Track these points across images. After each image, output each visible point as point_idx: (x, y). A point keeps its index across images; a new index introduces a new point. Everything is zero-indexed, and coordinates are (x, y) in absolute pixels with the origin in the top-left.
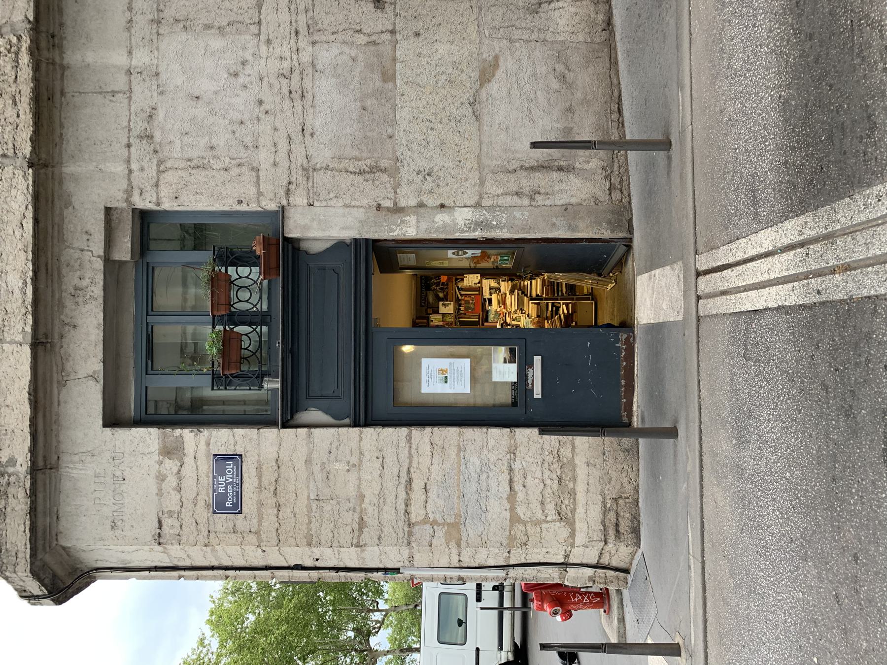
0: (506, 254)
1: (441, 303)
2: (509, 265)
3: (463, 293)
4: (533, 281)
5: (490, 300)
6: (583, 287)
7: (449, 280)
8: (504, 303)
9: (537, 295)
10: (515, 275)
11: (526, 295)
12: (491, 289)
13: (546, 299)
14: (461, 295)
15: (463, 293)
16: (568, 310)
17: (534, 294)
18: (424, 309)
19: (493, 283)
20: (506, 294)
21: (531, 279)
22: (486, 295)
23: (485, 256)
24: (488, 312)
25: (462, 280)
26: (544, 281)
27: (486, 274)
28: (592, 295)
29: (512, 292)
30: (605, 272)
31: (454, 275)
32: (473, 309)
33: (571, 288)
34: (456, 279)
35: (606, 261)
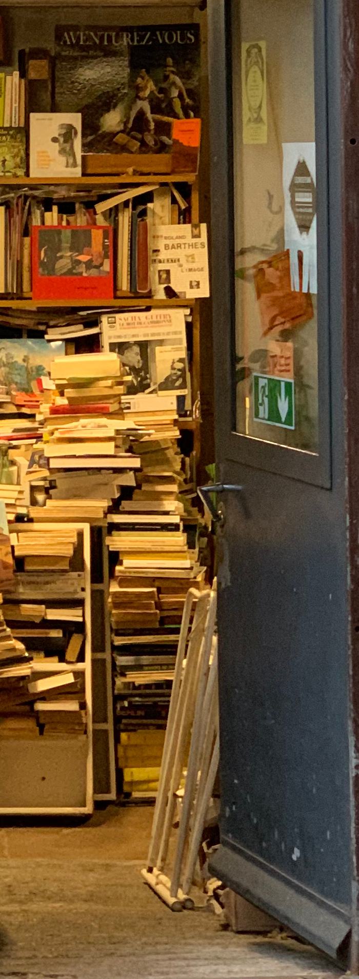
0: (300, 414)
1: (75, 120)
2: (252, 423)
3: (125, 220)
4: (180, 538)
5: (90, 345)
6: (155, 760)
7: (184, 157)
8: (75, 410)
9: (115, 558)
10: (207, 457)
11: (115, 508)
12: (144, 346)
13: (98, 597)
14: (113, 213)
15: (125, 220)
16: (46, 696)
17: (117, 542)
18: (51, 47)
19: (169, 357)
20: (119, 414)
21: (189, 528)
22: (113, 329)
23: (290, 313)
24: (38, 335)
25: (184, 216)
26: (182, 585)
27: (212, 323)
28: (118, 801)
29: (131, 443)
30: (221, 854)
31: (204, 179)
32: (49, 266)
33: (150, 709)
34: (184, 189)
35: (270, 856)
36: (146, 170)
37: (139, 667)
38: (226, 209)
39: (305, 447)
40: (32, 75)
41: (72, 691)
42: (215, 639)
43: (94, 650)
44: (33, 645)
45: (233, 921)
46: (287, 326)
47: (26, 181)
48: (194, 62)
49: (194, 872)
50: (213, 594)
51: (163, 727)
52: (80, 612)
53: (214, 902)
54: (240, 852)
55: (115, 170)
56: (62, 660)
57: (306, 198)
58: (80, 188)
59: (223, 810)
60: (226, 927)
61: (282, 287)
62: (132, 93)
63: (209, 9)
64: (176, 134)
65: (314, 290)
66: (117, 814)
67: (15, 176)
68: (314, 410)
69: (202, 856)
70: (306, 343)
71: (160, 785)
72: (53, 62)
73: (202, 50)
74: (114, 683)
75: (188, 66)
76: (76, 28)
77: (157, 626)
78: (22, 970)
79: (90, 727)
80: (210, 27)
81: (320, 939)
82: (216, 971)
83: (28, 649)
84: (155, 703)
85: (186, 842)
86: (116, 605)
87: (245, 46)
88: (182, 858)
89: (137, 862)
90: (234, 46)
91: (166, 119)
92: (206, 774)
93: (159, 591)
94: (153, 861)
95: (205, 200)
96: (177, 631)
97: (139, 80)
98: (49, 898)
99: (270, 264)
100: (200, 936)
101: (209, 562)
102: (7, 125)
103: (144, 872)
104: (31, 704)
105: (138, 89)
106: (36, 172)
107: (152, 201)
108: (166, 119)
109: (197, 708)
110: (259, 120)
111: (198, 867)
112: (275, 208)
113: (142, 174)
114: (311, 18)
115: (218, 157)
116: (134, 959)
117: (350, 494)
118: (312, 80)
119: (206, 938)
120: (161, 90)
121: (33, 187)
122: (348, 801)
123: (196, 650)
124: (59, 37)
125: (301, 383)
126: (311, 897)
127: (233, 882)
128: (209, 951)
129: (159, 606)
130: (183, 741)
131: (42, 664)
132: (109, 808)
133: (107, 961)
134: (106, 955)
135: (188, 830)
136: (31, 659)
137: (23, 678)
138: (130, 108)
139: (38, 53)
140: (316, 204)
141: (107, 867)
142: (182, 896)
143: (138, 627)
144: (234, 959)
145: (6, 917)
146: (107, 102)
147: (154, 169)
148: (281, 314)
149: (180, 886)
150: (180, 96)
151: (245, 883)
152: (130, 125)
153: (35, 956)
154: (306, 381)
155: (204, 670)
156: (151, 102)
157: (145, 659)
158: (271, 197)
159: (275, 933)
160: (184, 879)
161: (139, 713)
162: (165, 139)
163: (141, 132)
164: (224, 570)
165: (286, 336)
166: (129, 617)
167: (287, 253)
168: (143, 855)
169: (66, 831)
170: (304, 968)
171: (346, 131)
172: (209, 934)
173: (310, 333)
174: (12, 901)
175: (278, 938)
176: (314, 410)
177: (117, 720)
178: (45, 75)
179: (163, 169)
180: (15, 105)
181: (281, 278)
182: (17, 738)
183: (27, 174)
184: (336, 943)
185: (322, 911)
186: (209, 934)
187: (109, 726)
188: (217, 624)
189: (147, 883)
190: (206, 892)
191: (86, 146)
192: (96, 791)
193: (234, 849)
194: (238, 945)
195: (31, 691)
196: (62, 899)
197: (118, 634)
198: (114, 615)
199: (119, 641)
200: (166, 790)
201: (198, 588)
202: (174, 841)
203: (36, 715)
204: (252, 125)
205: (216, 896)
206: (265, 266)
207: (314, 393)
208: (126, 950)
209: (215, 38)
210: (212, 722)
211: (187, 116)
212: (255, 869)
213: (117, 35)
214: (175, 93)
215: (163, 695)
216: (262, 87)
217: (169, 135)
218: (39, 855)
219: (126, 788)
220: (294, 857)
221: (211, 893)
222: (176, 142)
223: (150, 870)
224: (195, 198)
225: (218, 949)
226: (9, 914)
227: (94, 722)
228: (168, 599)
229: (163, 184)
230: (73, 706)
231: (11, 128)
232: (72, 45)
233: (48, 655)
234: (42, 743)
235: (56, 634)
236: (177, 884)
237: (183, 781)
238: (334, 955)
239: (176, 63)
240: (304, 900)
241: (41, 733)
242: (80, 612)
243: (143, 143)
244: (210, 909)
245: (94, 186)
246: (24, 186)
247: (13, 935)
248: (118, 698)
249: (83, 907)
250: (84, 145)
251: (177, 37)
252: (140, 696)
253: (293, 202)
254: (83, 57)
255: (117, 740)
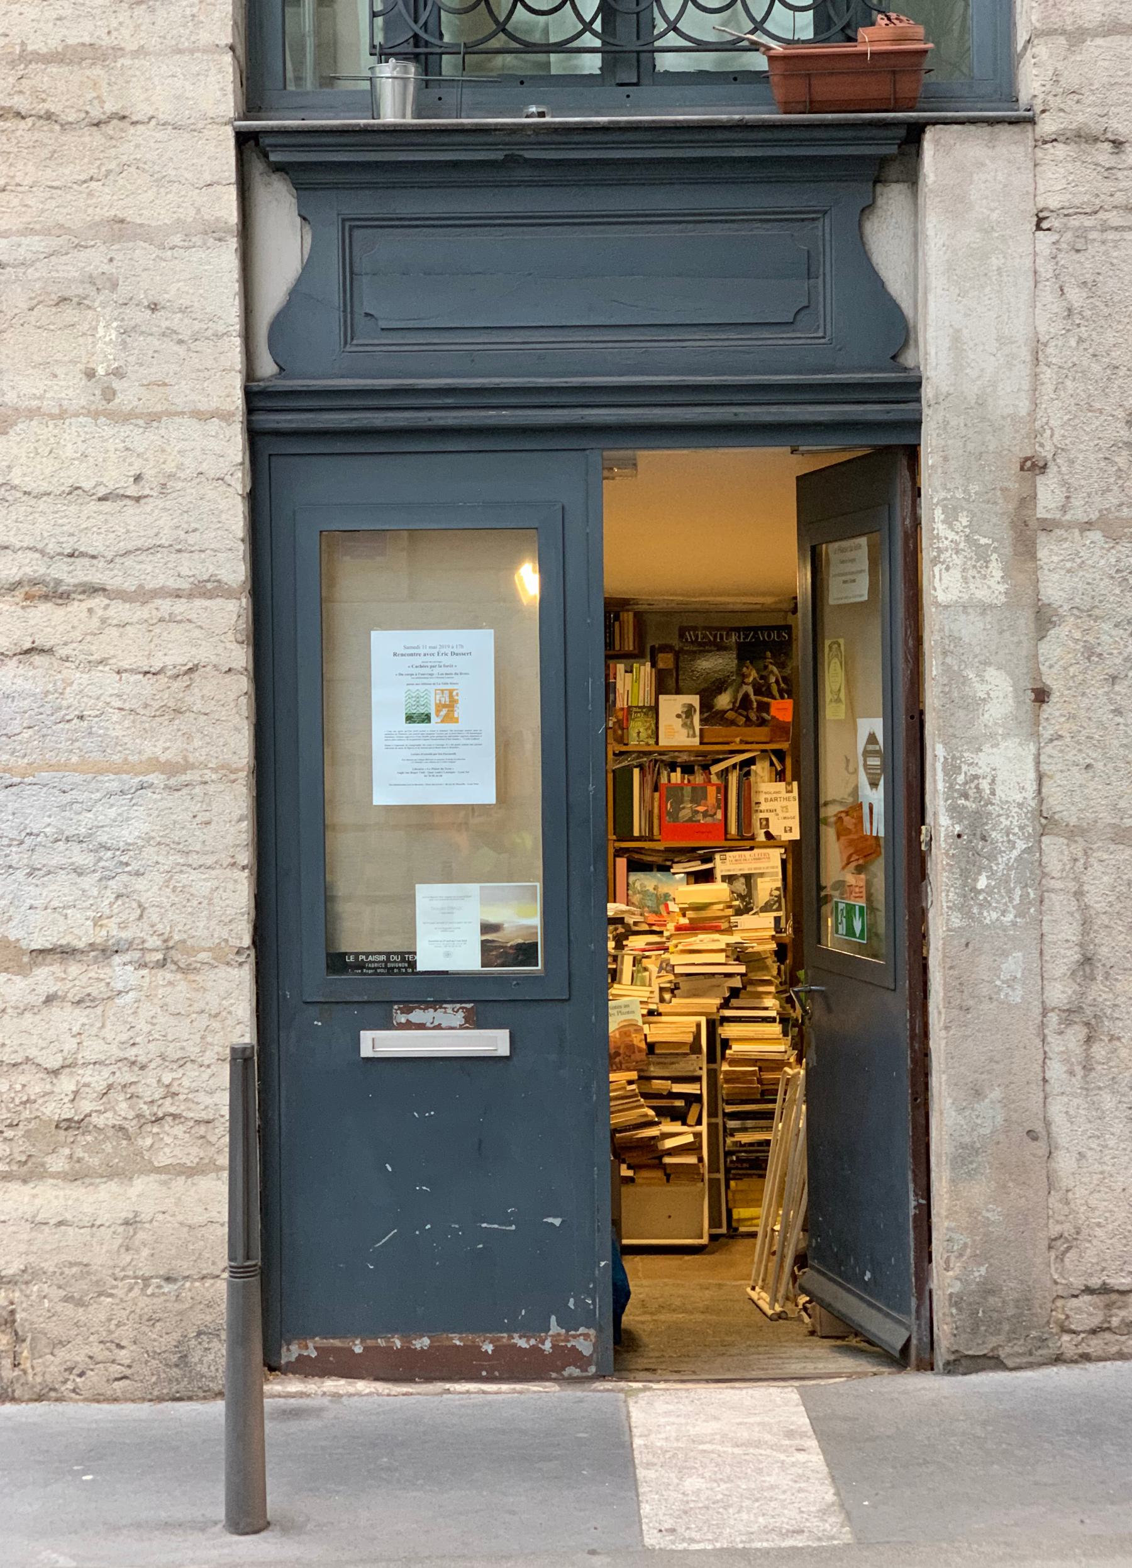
0: (871, 931)
1: (695, 700)
2: (834, 938)
3: (733, 779)
4: (776, 1029)
5: (706, 877)
6: (757, 1203)
7: (780, 730)
8: (694, 928)
9: (726, 1044)
10: (798, 965)
11: (725, 1004)
12: (748, 878)
13: (712, 1074)
14: (724, 774)
15: (733, 779)
16: (671, 1152)
17: (727, 1031)
18: (676, 643)
19: (768, 886)
20: (729, 931)
21: (784, 1020)
22: (724, 864)
23: (863, 853)
24: (665, 869)
25: (780, 776)
26: (778, 1065)
27: (802, 859)
28: (728, 1234)
29: (739, 954)
30: (809, 1276)
31: (795, 747)
32: (674, 815)
33: (753, 1163)
34: (780, 755)
35: (848, 1278)
36: (750, 739)
37: (744, 1130)
38: (813, 769)
39: (874, 956)
40: (661, 665)
41: (692, 1148)
42: (804, 1107)
43: (709, 1116)
44: (661, 1112)
45: (818, 1328)
46: (861, 862)
47: (656, 748)
48: (788, 655)
49: (787, 1290)
50: (802, 1072)
51: (763, 1176)
52: (698, 1086)
53: (803, 1313)
54: (824, 1274)
55: (725, 740)
56: (684, 1123)
57: (875, 762)
58: (699, 754)
59: (810, 1242)
60: (812, 1333)
61: (857, 832)
62: (739, 679)
63: (799, 614)
64: (773, 712)
65: (882, 834)
66: (727, 1245)
67: (648, 744)
68: (882, 928)
69: (794, 1277)
70: (875, 876)
71: (761, 1222)
72: (677, 655)
73: (794, 646)
74: (725, 1142)
75: (783, 658)
76: (695, 628)
77: (759, 1097)
78: (653, 1367)
79: (706, 1177)
80: (800, 627)
81: (886, 1342)
82: (804, 1368)
83: (657, 1115)
84: (757, 1157)
85: (781, 1266)
86: (727, 1081)
87: (827, 643)
88: (778, 1279)
89: (743, 1282)
90: (819, 642)
91: (766, 699)
92: (797, 1213)
93: (760, 1069)
94: (756, 1281)
95: (796, 763)
96: (774, 1101)
97: (745, 669)
98: (674, 1310)
99: (847, 813)
100: (792, 1340)
101: (799, 1047)
102: (641, 704)
103: (749, 1290)
104: (660, 1158)
105: (744, 676)
106: (664, 742)
107: (754, 764)
108: (766, 699)
109: (790, 1161)
110: (838, 700)
111: (791, 1286)
112: (851, 769)
113: (747, 743)
114: (880, 620)
115: (807, 730)
116: (740, 1358)
117: (910, 994)
118: (880, 669)
119: (797, 1341)
120: (762, 677)
121: (661, 753)
122: (908, 1234)
123: (789, 1116)
124: (682, 636)
125: (871, 907)
126: (879, 1310)
127: (818, 1298)
128: (799, 1352)
129: (760, 1081)
130: (779, 1187)
131: (668, 1127)
132: (722, 1240)
133: (720, 1360)
134: (719, 1355)
135: (783, 1257)
136: (660, 1123)
137: (654, 1138)
138: (737, 691)
139: (665, 648)
140: (884, 763)
141: (720, 1286)
142: (778, 1308)
143: (744, 1098)
144: (819, 1358)
145: (640, 1326)
146: (719, 686)
147: (756, 739)
148: (855, 852)
149: (777, 1301)
150: (777, 682)
151: (828, 1299)
152: (737, 705)
153: (663, 1356)
154: (875, 905)
155: (795, 1132)
156: (754, 686)
157: (750, 1123)
158: (848, 761)
159: (851, 1338)
160: (780, 1295)
161: (745, 1165)
162: (765, 715)
163: (746, 709)
164: (812, 1053)
165: (859, 869)
166: (737, 1090)
167: (861, 805)
168: (748, 1277)
169: (687, 1258)
170: (873, 1365)
171: (907, 710)
172: (799, 1338)
173: (879, 867)
174: (645, 1313)
175: (854, 1342)
176: (882, 928)
177: (727, 1171)
178: (671, 665)
179: (763, 739)
180: (648, 689)
181: (856, 824)
182: (649, 1185)
183: (657, 743)
184: (899, 1345)
185: (888, 1320)
186: (799, 1338)
187: (721, 1176)
188: (806, 1095)
189: (750, 1299)
190: (797, 1305)
191: (703, 721)
192: (710, 1227)
193: (819, 1271)
194: (822, 1347)
195: (660, 1148)
196: (685, 1311)
197: (728, 1104)
198: (725, 1088)
199: (729, 1109)
200: (766, 1226)
201: (791, 1068)
202: (773, 1265)
203: (664, 1167)
204: (833, 704)
205: (805, 1309)
206: (843, 815)
207: (881, 916)
208: (734, 1351)
209: (804, 637)
210: (802, 1172)
211: (782, 697)
212: (835, 1287)
213: (727, 634)
214: (773, 680)
215: (763, 1151)
216: (841, 675)
217: (768, 713)
218: (666, 1277)
219: (734, 1224)
220: (866, 1278)
221: (801, 1306)
222: (773, 718)
223: (753, 1289)
224: (788, 762)
225: (806, 1350)
226: (643, 1323)
227: (709, 1172)
228: (768, 1076)
229: (763, 751)
230: (692, 1160)
231: (644, 707)
232: (692, 642)
233: (673, 1119)
234: (669, 1189)
235: (679, 1103)
236: (775, 1299)
237: (779, 1219)
238: (897, 1355)
239: (773, 656)
240: (874, 1312)
241: (668, 1180)
242: (698, 1086)
243: (748, 719)
244: (800, 1319)
245: (710, 752)
246: (654, 752)
247: (645, 1339)
248: (728, 1154)
249: (700, 1317)
250: (701, 720)
251: (774, 636)
252: (745, 1152)
253: (865, 765)
254: (701, 651)
255: (727, 1186)
